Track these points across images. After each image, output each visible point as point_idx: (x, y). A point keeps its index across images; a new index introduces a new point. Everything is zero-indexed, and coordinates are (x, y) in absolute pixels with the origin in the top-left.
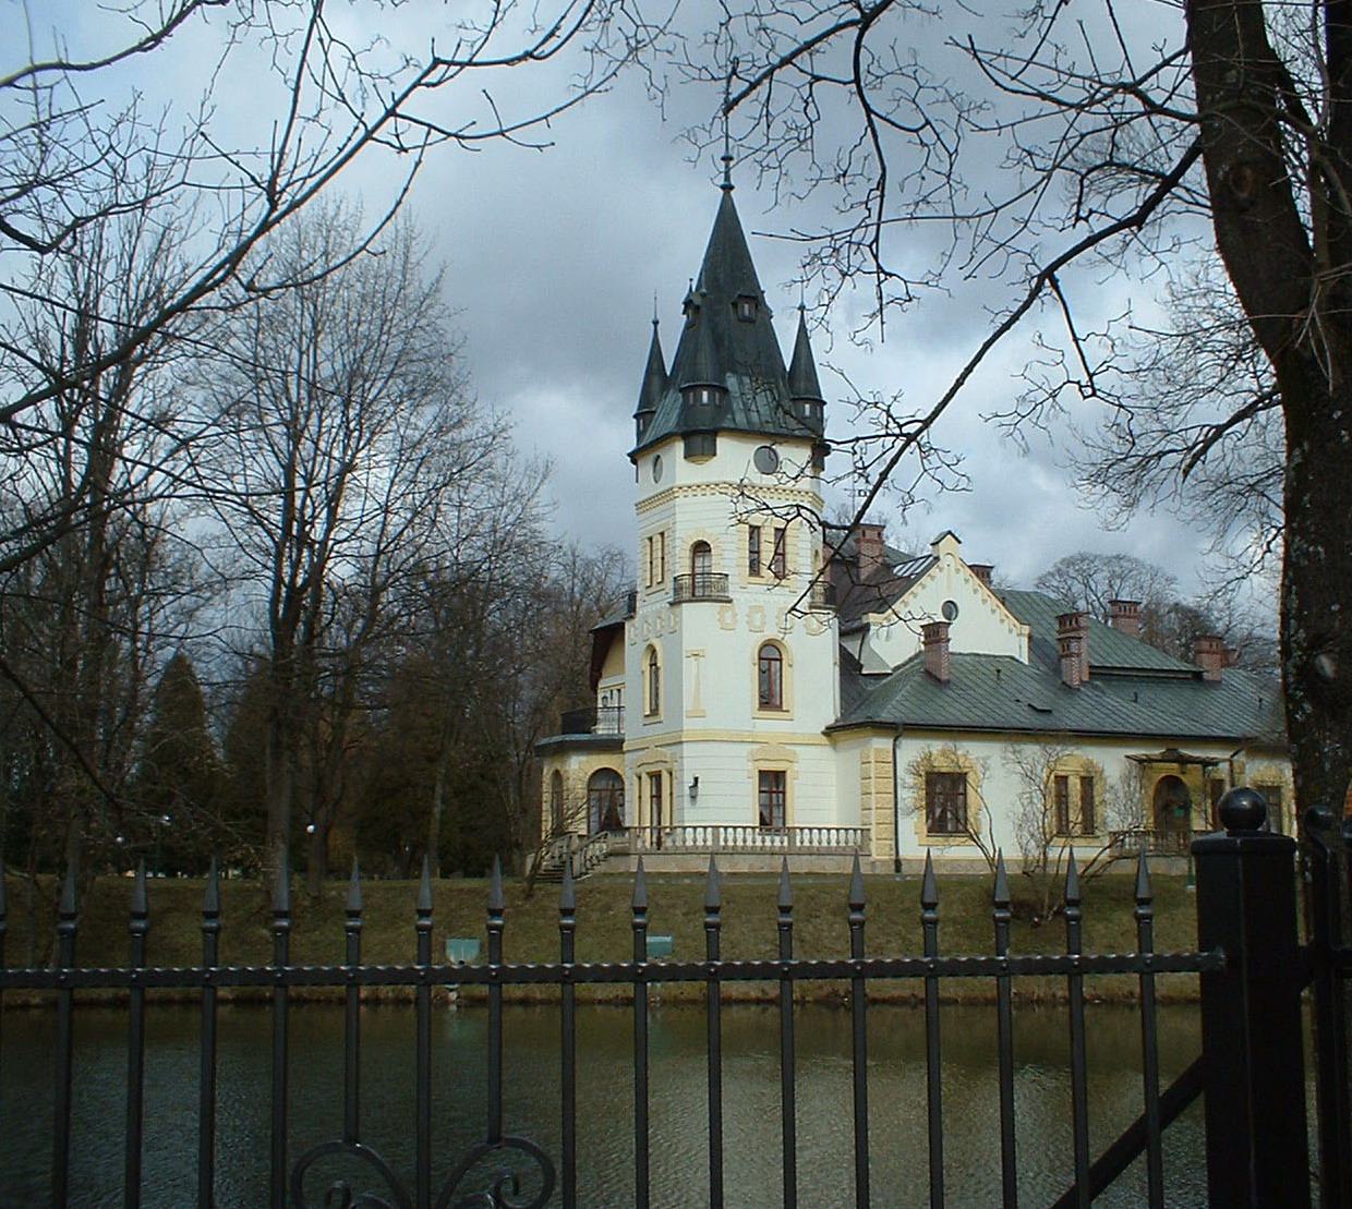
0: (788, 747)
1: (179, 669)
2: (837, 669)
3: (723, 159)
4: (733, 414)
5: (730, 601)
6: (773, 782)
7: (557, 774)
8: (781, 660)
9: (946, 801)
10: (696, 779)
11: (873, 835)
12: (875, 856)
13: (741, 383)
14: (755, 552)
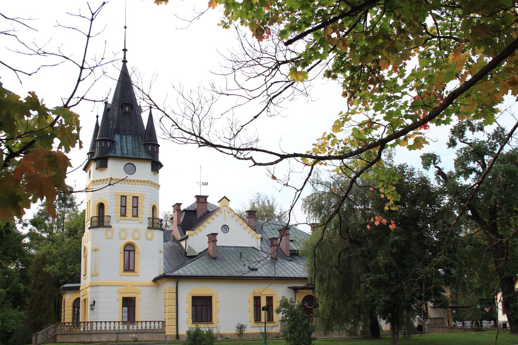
0: (136, 287)
2: (162, 254)
3: (123, 50)
4: (115, 150)
5: (111, 227)
6: (129, 303)
8: (134, 251)
9: (202, 307)
10: (94, 302)
11: (167, 324)
12: (167, 333)
13: (121, 138)
14: (124, 207)
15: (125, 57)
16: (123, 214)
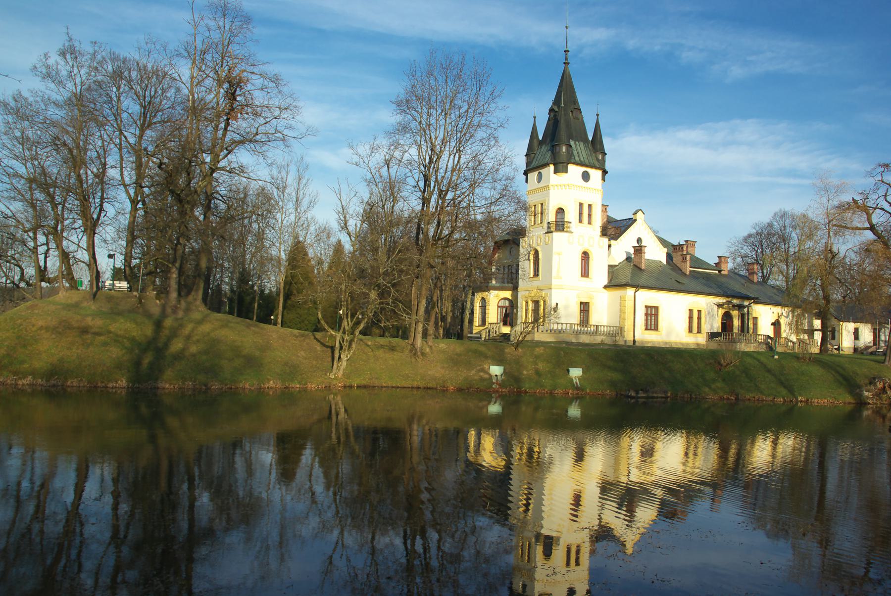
1: (298, 252)
6: (585, 308)
7: (483, 299)
14: (581, 214)
15: (566, 59)
16: (581, 221)
